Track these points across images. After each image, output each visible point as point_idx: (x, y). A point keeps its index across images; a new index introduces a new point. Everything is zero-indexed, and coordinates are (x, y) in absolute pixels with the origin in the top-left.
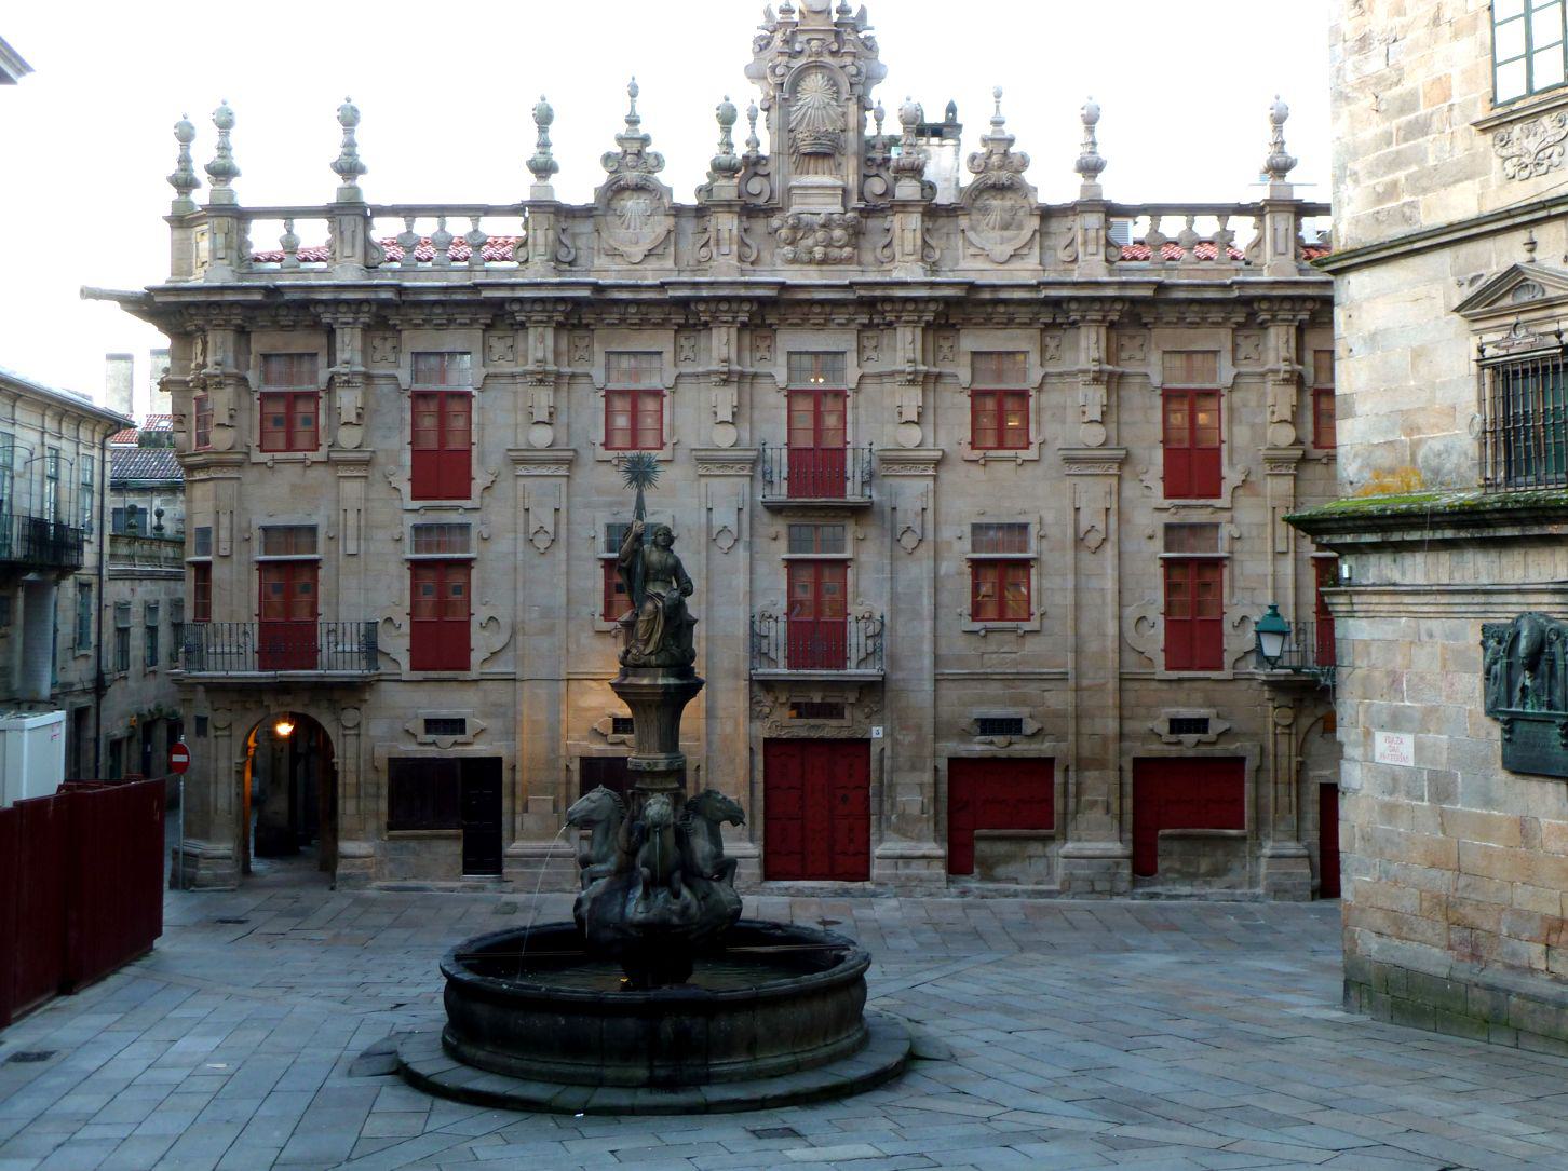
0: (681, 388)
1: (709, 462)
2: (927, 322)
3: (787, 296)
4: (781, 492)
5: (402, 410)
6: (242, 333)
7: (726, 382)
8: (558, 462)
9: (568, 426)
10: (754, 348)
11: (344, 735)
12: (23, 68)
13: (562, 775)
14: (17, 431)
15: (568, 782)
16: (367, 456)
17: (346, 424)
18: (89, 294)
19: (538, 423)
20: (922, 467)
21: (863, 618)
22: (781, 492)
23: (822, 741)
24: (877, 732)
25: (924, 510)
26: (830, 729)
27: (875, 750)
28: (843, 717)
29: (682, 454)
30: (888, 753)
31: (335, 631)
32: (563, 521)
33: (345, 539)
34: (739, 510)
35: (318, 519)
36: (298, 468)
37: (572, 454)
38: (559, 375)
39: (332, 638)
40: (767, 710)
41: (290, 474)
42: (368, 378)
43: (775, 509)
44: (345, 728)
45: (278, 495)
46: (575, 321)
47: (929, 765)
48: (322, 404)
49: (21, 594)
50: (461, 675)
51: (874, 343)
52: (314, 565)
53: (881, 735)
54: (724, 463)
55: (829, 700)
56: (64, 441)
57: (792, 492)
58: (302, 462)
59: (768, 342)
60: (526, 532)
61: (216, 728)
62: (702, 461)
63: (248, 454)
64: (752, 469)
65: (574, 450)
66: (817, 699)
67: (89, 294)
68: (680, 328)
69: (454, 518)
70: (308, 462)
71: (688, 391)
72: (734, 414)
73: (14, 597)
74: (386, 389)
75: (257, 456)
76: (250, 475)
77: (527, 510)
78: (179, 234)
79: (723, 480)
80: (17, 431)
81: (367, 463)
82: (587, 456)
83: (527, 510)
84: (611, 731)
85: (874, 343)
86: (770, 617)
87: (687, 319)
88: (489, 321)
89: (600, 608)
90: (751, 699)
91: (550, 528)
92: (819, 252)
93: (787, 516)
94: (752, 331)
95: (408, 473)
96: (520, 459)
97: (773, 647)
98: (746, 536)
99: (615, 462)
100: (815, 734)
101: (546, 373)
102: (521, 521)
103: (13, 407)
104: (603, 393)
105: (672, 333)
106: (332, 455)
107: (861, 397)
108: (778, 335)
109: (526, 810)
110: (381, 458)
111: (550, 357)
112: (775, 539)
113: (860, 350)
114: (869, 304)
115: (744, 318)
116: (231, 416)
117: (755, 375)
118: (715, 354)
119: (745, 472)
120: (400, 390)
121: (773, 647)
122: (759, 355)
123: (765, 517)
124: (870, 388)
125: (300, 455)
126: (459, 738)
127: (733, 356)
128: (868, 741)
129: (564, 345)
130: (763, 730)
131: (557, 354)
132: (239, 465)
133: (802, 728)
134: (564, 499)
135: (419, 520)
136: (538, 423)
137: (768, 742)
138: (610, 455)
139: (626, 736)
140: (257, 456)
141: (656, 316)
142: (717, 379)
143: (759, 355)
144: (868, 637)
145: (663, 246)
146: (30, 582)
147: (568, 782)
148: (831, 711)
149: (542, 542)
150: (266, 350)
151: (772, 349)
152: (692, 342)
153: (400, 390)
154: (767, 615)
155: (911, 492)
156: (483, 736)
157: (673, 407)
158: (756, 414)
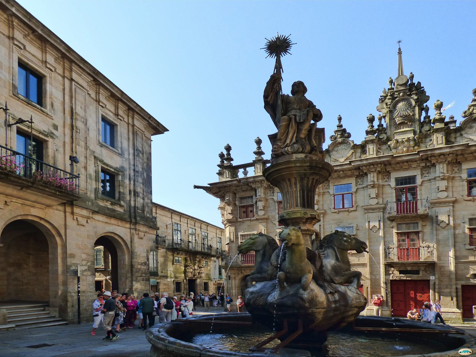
5: (275, 206)
9: (323, 205)
24: (432, 278)
27: (431, 283)
28: (419, 274)
30: (437, 283)
36: (249, 222)
41: (248, 223)
47: (454, 287)
48: (254, 207)
51: (427, 172)
53: (434, 279)
58: (250, 220)
59: (388, 177)
62: (365, 209)
68: (357, 177)
71: (361, 193)
75: (239, 220)
79: (374, 214)
85: (427, 172)
105: (355, 178)
113: (422, 174)
115: (379, 169)
117: (383, 185)
120: (275, 202)
122: (384, 180)
123: (389, 222)
124: (426, 184)
125: (250, 219)
127: (376, 180)
128: (429, 281)
138: (336, 211)
143: (384, 180)
148: (417, 272)
152: (362, 180)
153: (275, 202)
158: (384, 196)
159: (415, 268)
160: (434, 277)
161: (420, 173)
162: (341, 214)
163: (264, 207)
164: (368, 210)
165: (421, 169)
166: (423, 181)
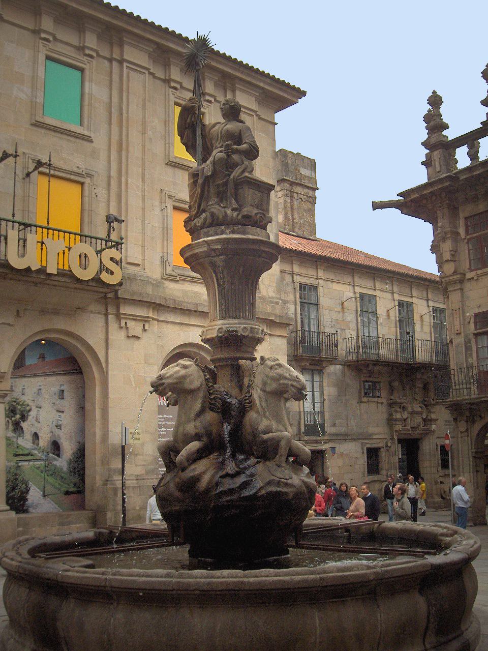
12: (303, 94)
18: (377, 206)
67: (377, 206)
76: (468, 286)
116: (453, 255)
132: (461, 282)
140: (469, 275)
150: (467, 215)
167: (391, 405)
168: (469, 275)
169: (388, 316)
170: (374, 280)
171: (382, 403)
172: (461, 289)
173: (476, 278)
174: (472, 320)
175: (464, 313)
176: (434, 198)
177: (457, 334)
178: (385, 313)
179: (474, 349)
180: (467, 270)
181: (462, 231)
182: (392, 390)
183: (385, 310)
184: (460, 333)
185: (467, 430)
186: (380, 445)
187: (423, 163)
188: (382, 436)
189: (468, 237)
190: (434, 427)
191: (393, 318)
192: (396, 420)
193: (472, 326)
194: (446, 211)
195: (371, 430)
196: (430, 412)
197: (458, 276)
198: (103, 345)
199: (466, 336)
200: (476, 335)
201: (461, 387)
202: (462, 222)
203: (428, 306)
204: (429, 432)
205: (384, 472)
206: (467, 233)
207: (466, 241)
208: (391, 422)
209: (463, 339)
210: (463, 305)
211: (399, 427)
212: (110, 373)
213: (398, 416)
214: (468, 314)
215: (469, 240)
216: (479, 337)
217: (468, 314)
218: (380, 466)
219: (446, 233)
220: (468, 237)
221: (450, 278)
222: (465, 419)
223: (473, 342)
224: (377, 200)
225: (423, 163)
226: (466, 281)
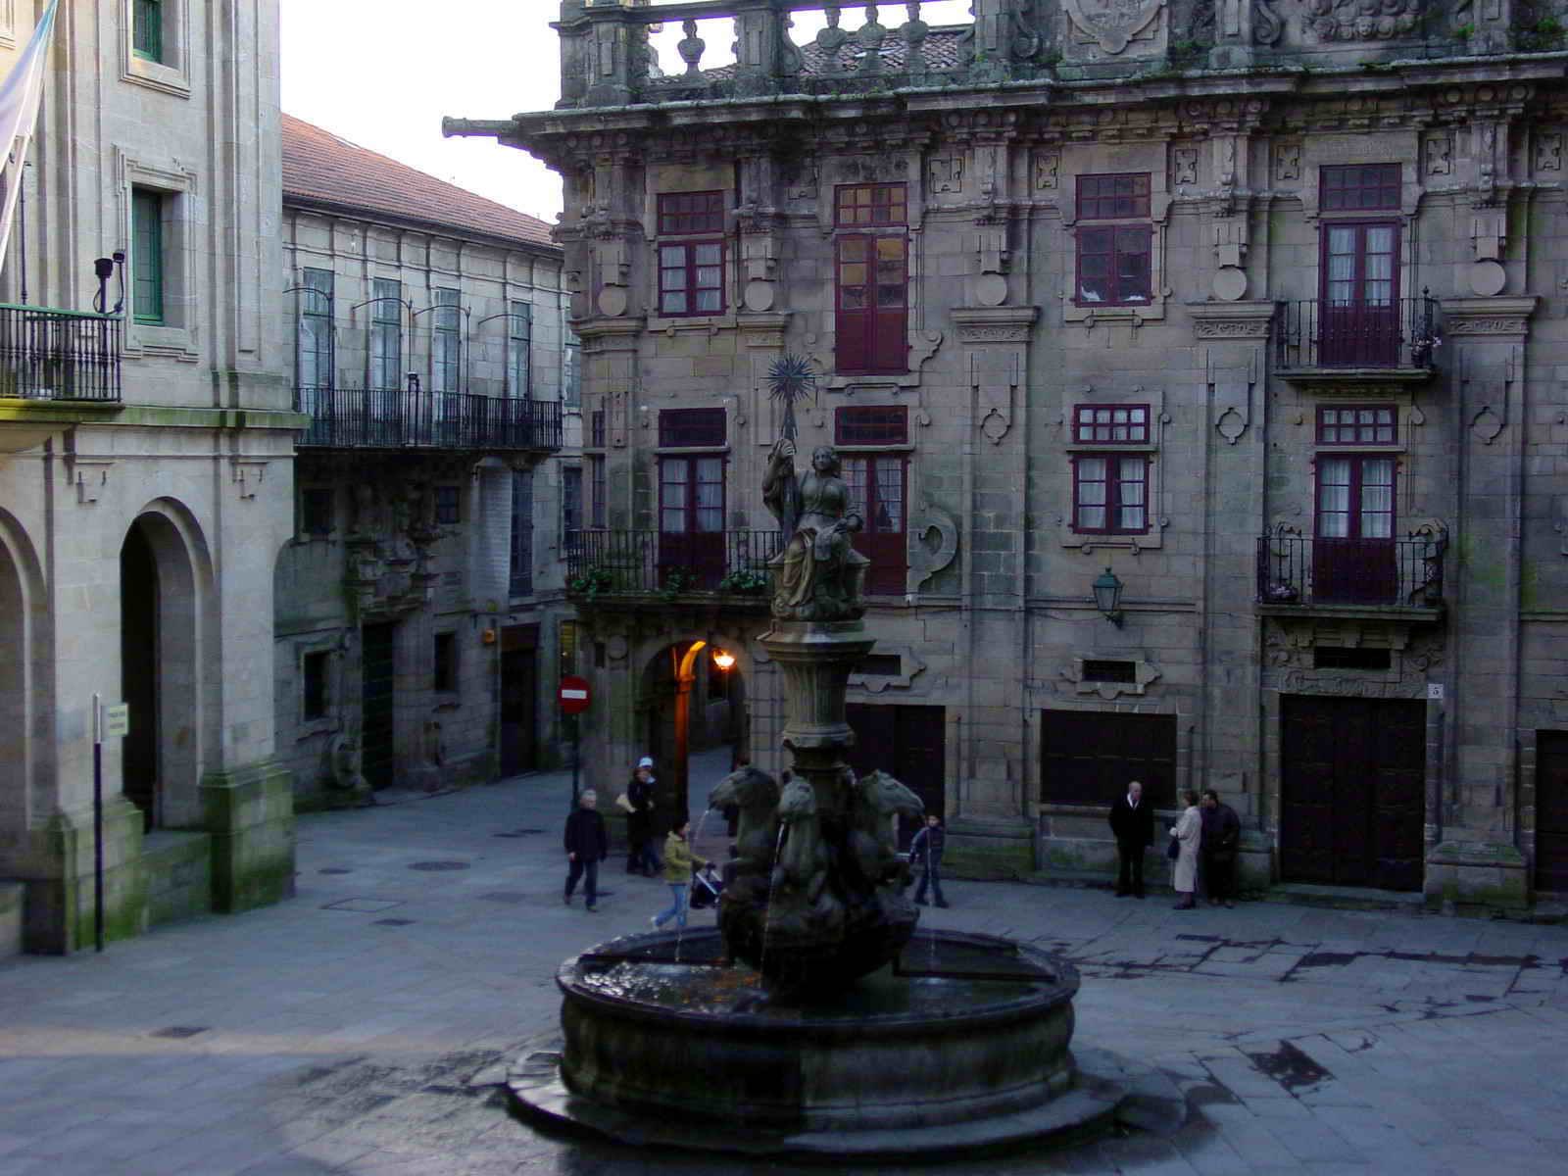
0: (1177, 219)
1: (1209, 322)
2: (1514, 116)
3: (1309, 90)
4: (1308, 363)
6: (634, 170)
7: (1230, 212)
8: (1015, 324)
10: (1274, 161)
11: (756, 672)
13: (1016, 733)
14: (464, 285)
15: (1025, 742)
16: (780, 320)
17: (754, 279)
19: (986, 273)
20: (1506, 323)
21: (1419, 534)
22: (1308, 363)
23: (1357, 700)
24: (1435, 692)
25: (1508, 384)
26: (1369, 684)
29: (1176, 314)
31: (746, 543)
32: (1021, 400)
33: (756, 425)
34: (1251, 386)
35: (725, 402)
36: (703, 337)
37: (1030, 312)
38: (1014, 210)
39: (742, 550)
40: (1283, 656)
41: (694, 342)
42: (781, 219)
43: (1301, 385)
44: (757, 663)
45: (675, 374)
46: (1035, 136)
49: (476, 484)
50: (896, 600)
51: (1444, 149)
52: (723, 457)
53: (1441, 696)
54: (1229, 322)
55: (1367, 645)
56: (535, 292)
57: (1323, 360)
58: (706, 328)
59: (1293, 154)
60: (974, 418)
61: (612, 659)
63: (645, 319)
64: (1269, 330)
65: (1038, 309)
66: (1350, 642)
69: (883, 398)
70: (714, 330)
72: (1242, 256)
73: (468, 488)
74: (804, 233)
75: (655, 324)
76: (648, 347)
77: (976, 388)
78: (569, 43)
80: (464, 285)
81: (784, 329)
82: (1052, 317)
83: (976, 388)
84: (1080, 676)
86: (1291, 531)
87: (1180, 128)
88: (927, 141)
89: (1068, 518)
90: (1263, 640)
91: (1004, 412)
92: (1363, 24)
93: (1315, 394)
94: (1271, 140)
95: (830, 341)
96: (972, 326)
97: (1296, 572)
98: (1259, 419)
99: (1088, 322)
100: (1348, 691)
101: (997, 208)
102: (968, 402)
103: (458, 255)
104: (1073, 231)
106: (740, 319)
107: (1424, 226)
108: (1308, 143)
109: (972, 775)
110: (799, 322)
111: (1002, 184)
112: (1300, 424)
114: (1430, 94)
116: (623, 274)
118: (1217, 172)
119: (1260, 334)
121: (1296, 572)
122: (1282, 172)
126: (894, 680)
129: (1022, 171)
130: (1282, 682)
131: (1012, 179)
132: (636, 335)
133: (1332, 682)
134: (1023, 375)
135: (842, 401)
136: (986, 273)
137: (1285, 699)
138: (1083, 313)
139: (1099, 684)
141: (1141, 121)
142: (1218, 208)
144: (1426, 560)
145: (1154, 26)
146: (484, 469)
147: (1025, 742)
148: (1379, 660)
149: (995, 429)
150: (664, 189)
151: (1301, 162)
154: (1286, 528)
155: (1494, 354)
156: (921, 682)
157: (1165, 248)
159: (1374, 643)
160: (1441, 688)
161: (1415, 155)
162: (1102, 331)
163: (776, 264)
164: (1209, 322)
165: (1421, 137)
166: (1423, 198)
167: (351, 546)
168: (655, 324)
169: (353, 321)
170: (332, 226)
171: (334, 543)
172: (635, 351)
173: (670, 332)
174: (655, 423)
175: (636, 405)
176: (597, 142)
177: (616, 447)
178: (347, 317)
179: (655, 483)
180: (650, 311)
181: (648, 220)
182: (354, 511)
183: (347, 308)
184: (623, 447)
185: (625, 657)
186: (331, 645)
187: (553, 25)
188: (332, 624)
189: (662, 238)
190: (430, 593)
191: (361, 326)
192: (366, 583)
193: (653, 436)
194: (618, 171)
195: (316, 609)
196: (425, 557)
197: (632, 324)
198: (41, 522)
199: (638, 456)
200: (662, 458)
201: (623, 563)
202: (649, 201)
203: (428, 287)
204: (419, 605)
205: (333, 711)
206: (660, 231)
207: (655, 246)
208: (350, 586)
209: (630, 461)
210: (634, 387)
211: (368, 600)
212: (57, 587)
213: (368, 573)
214: (644, 408)
215: (662, 245)
216: (667, 464)
217: (644, 408)
218: (326, 694)
219: (614, 224)
220: (662, 238)
221: (614, 323)
222: (624, 633)
223: (654, 471)
224: (457, 115)
225: (553, 25)
226: (645, 334)
